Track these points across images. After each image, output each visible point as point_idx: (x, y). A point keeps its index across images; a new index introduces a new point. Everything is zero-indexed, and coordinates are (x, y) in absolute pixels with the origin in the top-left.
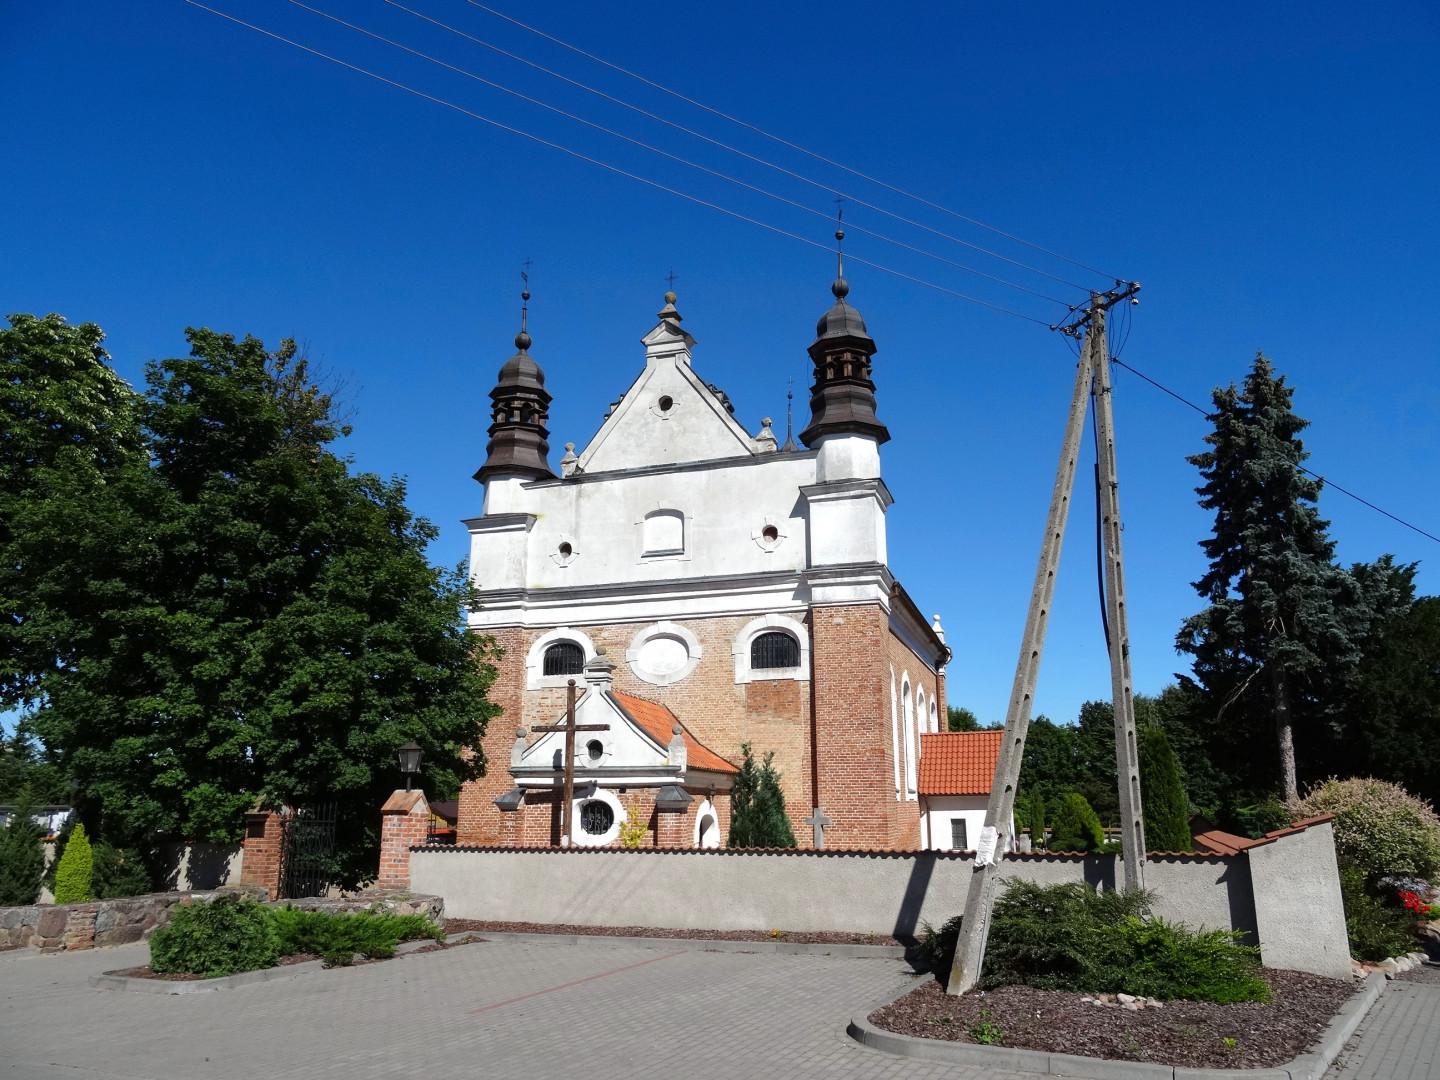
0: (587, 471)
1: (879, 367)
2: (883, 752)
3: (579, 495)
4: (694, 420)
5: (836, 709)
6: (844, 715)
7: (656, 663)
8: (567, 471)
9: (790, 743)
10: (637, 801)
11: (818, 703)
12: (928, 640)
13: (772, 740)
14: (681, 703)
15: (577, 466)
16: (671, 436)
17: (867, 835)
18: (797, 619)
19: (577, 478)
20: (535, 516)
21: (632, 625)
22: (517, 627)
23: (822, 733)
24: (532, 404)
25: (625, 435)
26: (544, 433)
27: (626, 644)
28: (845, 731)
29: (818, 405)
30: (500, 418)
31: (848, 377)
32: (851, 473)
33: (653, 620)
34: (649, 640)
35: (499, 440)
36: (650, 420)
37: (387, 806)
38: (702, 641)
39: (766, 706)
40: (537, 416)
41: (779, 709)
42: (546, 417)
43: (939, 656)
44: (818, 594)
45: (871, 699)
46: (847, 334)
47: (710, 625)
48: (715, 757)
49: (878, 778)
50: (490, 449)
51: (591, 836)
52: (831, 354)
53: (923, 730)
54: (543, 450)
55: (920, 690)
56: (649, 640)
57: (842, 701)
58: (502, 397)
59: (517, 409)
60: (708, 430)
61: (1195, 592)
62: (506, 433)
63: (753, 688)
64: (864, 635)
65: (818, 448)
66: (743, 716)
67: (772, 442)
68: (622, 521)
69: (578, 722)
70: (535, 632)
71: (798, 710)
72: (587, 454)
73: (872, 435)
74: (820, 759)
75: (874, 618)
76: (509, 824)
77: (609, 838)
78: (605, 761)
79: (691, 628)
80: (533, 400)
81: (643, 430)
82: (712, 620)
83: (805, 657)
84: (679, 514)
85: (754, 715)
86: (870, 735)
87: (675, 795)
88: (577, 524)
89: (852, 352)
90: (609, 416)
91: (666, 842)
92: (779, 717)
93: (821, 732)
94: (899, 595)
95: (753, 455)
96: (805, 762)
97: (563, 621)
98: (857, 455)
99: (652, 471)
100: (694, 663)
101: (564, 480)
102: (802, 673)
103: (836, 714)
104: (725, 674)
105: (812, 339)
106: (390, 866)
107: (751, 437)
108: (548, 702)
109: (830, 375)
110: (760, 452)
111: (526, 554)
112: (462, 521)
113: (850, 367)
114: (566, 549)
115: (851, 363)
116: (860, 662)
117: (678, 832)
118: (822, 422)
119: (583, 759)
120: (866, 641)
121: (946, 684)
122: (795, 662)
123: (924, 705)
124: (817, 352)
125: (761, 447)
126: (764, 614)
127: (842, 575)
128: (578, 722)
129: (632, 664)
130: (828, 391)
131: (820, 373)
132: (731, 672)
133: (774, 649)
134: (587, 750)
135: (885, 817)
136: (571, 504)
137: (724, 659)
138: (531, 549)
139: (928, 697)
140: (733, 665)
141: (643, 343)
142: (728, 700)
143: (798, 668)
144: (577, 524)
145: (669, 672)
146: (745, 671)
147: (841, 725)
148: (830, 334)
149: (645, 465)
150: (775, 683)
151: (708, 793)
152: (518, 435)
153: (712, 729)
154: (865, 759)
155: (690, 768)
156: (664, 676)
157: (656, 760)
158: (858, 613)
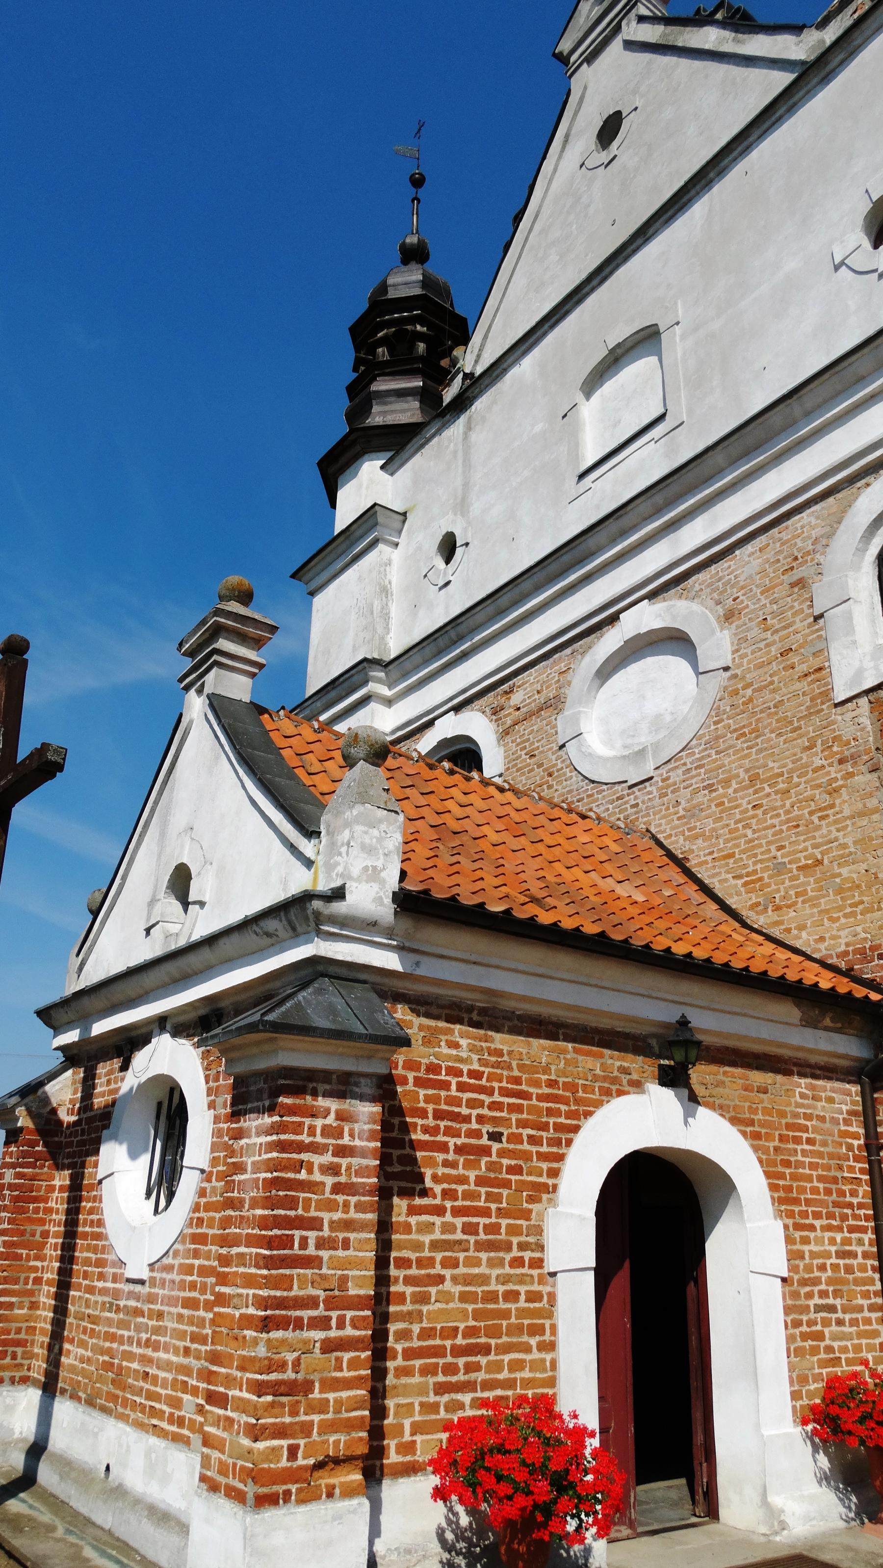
0: (479, 371)
14: (692, 812)
21: (568, 651)
24: (409, 327)
27: (554, 704)
33: (607, 618)
38: (729, 617)
40: (421, 347)
47: (748, 562)
59: (382, 342)
80: (413, 320)
82: (749, 548)
104: (803, 685)
136: (455, 452)
138: (395, 577)
142: (818, 762)
144: (466, 485)
153: (780, 869)
155: (413, 904)
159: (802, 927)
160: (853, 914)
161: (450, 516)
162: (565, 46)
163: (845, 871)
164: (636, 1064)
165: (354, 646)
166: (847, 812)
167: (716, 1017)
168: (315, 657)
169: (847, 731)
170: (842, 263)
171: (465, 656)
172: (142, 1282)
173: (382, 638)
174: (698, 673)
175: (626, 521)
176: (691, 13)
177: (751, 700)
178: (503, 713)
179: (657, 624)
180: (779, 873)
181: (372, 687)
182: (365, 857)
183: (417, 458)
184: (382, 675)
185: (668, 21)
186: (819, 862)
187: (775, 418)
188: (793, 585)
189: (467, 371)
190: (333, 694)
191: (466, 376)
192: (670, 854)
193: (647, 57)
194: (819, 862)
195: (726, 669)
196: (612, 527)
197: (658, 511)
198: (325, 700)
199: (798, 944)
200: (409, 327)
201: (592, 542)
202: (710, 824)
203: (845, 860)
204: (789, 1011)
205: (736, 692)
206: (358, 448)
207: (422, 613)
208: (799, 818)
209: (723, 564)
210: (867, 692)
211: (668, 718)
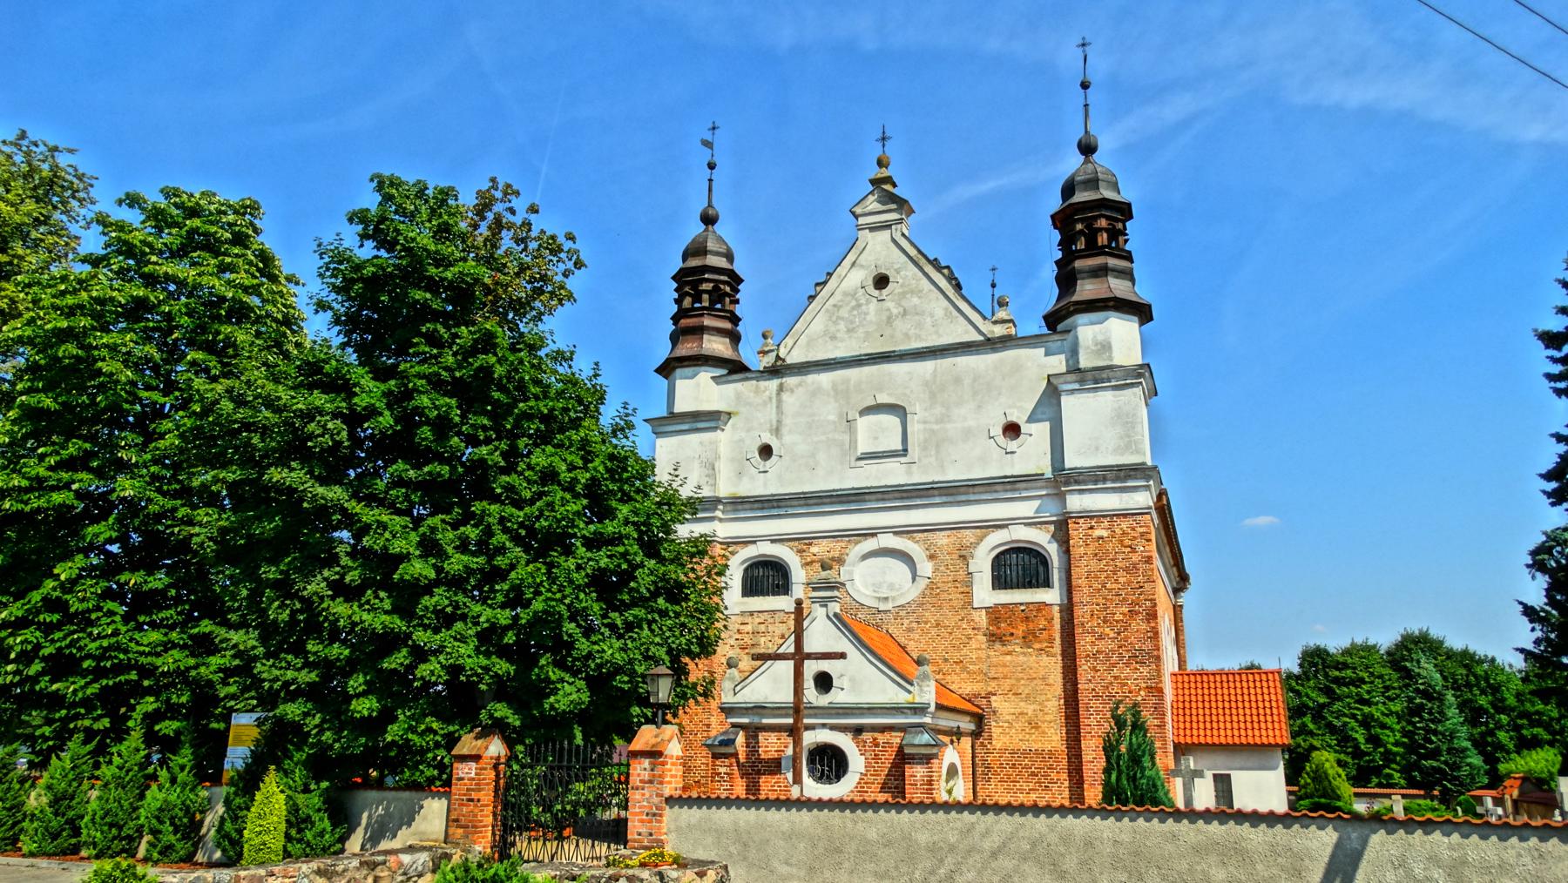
0: (789, 361)
1: (1136, 235)
3: (781, 389)
4: (915, 300)
5: (1101, 638)
6: (1113, 646)
7: (871, 581)
9: (1044, 679)
10: (877, 745)
11: (1078, 630)
14: (910, 630)
16: (889, 318)
19: (777, 370)
26: (735, 320)
27: (840, 561)
28: (1114, 665)
29: (1066, 279)
30: (687, 302)
31: (1104, 246)
33: (871, 533)
34: (865, 557)
36: (863, 301)
37: (638, 744)
38: (932, 557)
41: (1028, 639)
42: (737, 302)
44: (1076, 502)
45: (1144, 626)
46: (1098, 196)
47: (942, 539)
49: (1156, 722)
50: (675, 339)
52: (1081, 220)
54: (735, 338)
56: (865, 557)
58: (688, 280)
61: (1546, 501)
63: (995, 613)
64: (1134, 550)
68: (832, 417)
69: (807, 649)
71: (1051, 641)
72: (789, 341)
73: (1134, 314)
74: (1083, 698)
76: (722, 770)
77: (842, 789)
78: (836, 697)
83: (1056, 576)
85: (998, 646)
86: (1144, 670)
87: (925, 738)
88: (779, 422)
90: (812, 298)
91: (914, 794)
93: (1084, 668)
97: (764, 536)
100: (922, 584)
102: (1052, 596)
103: (1101, 645)
105: (1055, 203)
106: (642, 821)
107: (985, 318)
108: (749, 628)
109: (1081, 245)
114: (766, 451)
115: (1106, 230)
117: (930, 783)
118: (1075, 298)
119: (811, 694)
120: (1135, 558)
121: (1185, 614)
122: (1047, 584)
124: (1062, 220)
125: (999, 331)
126: (1005, 526)
127: (1104, 480)
128: (807, 649)
130: (1078, 264)
131: (1065, 244)
132: (968, 594)
133: (1020, 567)
137: (960, 578)
138: (724, 450)
141: (853, 213)
144: (779, 422)
145: (893, 594)
146: (985, 594)
147: (1108, 658)
148: (1080, 197)
151: (957, 734)
152: (708, 322)
153: (946, 660)
155: (940, 707)
156: (886, 599)
157: (901, 697)
162: (858, 210)
169: (977, 619)
171: (779, 516)
181: (718, 514)
182: (927, 694)
183: (739, 386)
185: (920, 252)
197: (902, 498)
207: (745, 479)
209: (930, 535)
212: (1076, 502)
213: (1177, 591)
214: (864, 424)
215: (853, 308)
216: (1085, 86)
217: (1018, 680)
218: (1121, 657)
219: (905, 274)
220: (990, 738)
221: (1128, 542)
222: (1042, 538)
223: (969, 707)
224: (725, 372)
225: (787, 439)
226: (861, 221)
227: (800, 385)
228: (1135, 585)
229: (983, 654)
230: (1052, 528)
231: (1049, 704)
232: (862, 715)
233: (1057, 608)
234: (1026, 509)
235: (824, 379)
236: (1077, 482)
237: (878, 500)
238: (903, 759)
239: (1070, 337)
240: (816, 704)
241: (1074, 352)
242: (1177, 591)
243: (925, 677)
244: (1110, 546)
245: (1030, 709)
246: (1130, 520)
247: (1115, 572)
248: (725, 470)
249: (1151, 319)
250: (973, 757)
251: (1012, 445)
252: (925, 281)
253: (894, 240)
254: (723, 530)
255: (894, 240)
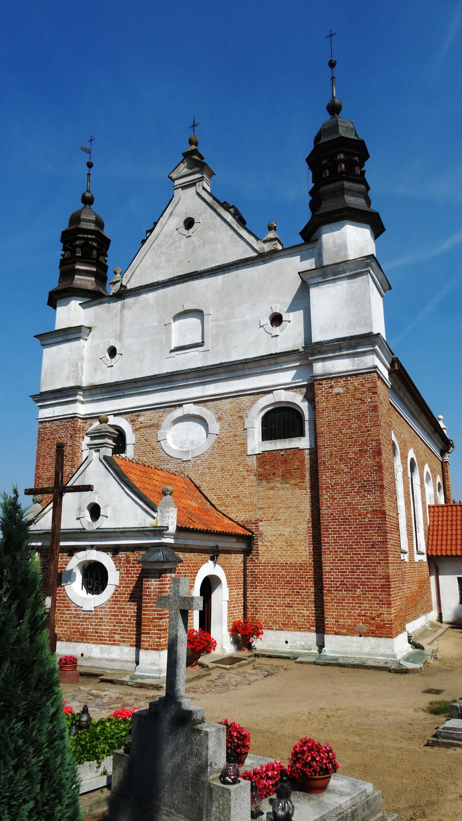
0: (129, 287)
2: (384, 513)
3: (123, 307)
4: (211, 233)
5: (337, 473)
7: (181, 440)
8: (113, 289)
10: (128, 562)
12: (433, 430)
13: (281, 505)
14: (203, 474)
15: (121, 284)
17: (370, 595)
18: (301, 394)
20: (90, 328)
21: (163, 410)
22: (73, 418)
23: (325, 496)
24: (90, 242)
25: (158, 254)
27: (157, 426)
28: (347, 494)
32: (347, 256)
33: (178, 404)
35: (67, 270)
36: (177, 239)
38: (219, 419)
39: (274, 474)
40: (95, 252)
41: (285, 478)
43: (446, 445)
44: (319, 368)
45: (370, 462)
47: (226, 404)
48: (230, 522)
51: (90, 595)
53: (430, 502)
55: (427, 468)
56: (176, 421)
57: (343, 466)
58: (68, 238)
59: (78, 246)
60: (223, 241)
62: (68, 266)
63: (263, 457)
64: (363, 402)
65: (318, 240)
66: (254, 484)
67: (277, 242)
68: (155, 324)
70: (89, 422)
72: (128, 273)
74: (325, 520)
75: (369, 385)
79: (209, 409)
81: (172, 248)
82: (227, 400)
84: (198, 313)
85: (264, 483)
86: (371, 497)
87: (159, 556)
88: (121, 330)
89: (345, 153)
92: (287, 483)
93: (325, 496)
94: (398, 372)
95: (261, 254)
96: (310, 525)
98: (353, 240)
99: (178, 279)
100: (213, 438)
101: (111, 296)
102: (303, 443)
103: (338, 478)
104: (239, 447)
107: (257, 239)
110: (266, 251)
111: (82, 358)
112: (35, 336)
113: (343, 166)
114: (112, 352)
116: (360, 427)
120: (364, 408)
123: (431, 482)
125: (267, 247)
126: (271, 392)
127: (340, 349)
129: (162, 443)
132: (244, 445)
133: (282, 421)
134: (87, 513)
135: (387, 578)
136: (116, 315)
138: (85, 353)
139: (435, 477)
140: (245, 439)
141: (171, 178)
142: (241, 470)
143: (303, 438)
144: (121, 330)
145: (193, 448)
146: (256, 443)
147: (343, 488)
149: (172, 276)
150: (282, 453)
152: (78, 267)
153: (228, 496)
154: (367, 520)
155: (180, 529)
156: (188, 452)
157: (148, 522)
158: (356, 382)
159: (232, 513)
160: (246, 512)
161: (114, 340)
162: (174, 176)
163: (245, 500)
164: (207, 556)
165: (67, 377)
166: (247, 485)
167: (223, 544)
168: (46, 374)
169: (250, 464)
170: (262, 326)
172: (92, 611)
173: (81, 377)
174: (207, 433)
175: (188, 376)
176: (222, 202)
177: (223, 446)
178: (135, 423)
179: (196, 413)
180: (227, 497)
182: (170, 519)
184: (82, 393)
185: (214, 198)
186: (238, 496)
187: (240, 367)
188: (239, 417)
189: (124, 284)
190: (59, 395)
191: (122, 285)
192: (195, 485)
193: (205, 205)
194: (238, 496)
195: (217, 435)
196: (184, 376)
197: (199, 377)
198: (54, 396)
199: (231, 517)
200: (90, 242)
201: (175, 378)
202: (208, 479)
203: (245, 497)
204: (234, 540)
205: (219, 442)
206: (70, 294)
207: (99, 373)
208: (234, 483)
209: (218, 402)
210: (256, 455)
211: (196, 442)
212: (319, 368)
213: (443, 453)
214: (175, 325)
215: (170, 245)
216: (332, 64)
217: (278, 509)
218: (353, 487)
219: (205, 216)
220: (257, 555)
221: (358, 395)
222: (297, 399)
223: (240, 531)
224: (90, 299)
225: (126, 341)
226: (177, 182)
227: (135, 303)
228: (364, 429)
229: (254, 490)
230: (304, 390)
231: (301, 527)
232: (117, 538)
233: (307, 452)
234: (286, 377)
235: (150, 296)
236: (321, 353)
237: (183, 380)
238: (146, 574)
239: (317, 245)
240: (88, 528)
241: (319, 257)
242: (443, 453)
243: (168, 505)
244: (345, 400)
245: (287, 531)
246: (360, 377)
247: (348, 421)
248: (86, 367)
249: (384, 230)
250: (245, 569)
251: (277, 330)
252: (218, 219)
253: (198, 194)
254: (82, 409)
255: (198, 194)
